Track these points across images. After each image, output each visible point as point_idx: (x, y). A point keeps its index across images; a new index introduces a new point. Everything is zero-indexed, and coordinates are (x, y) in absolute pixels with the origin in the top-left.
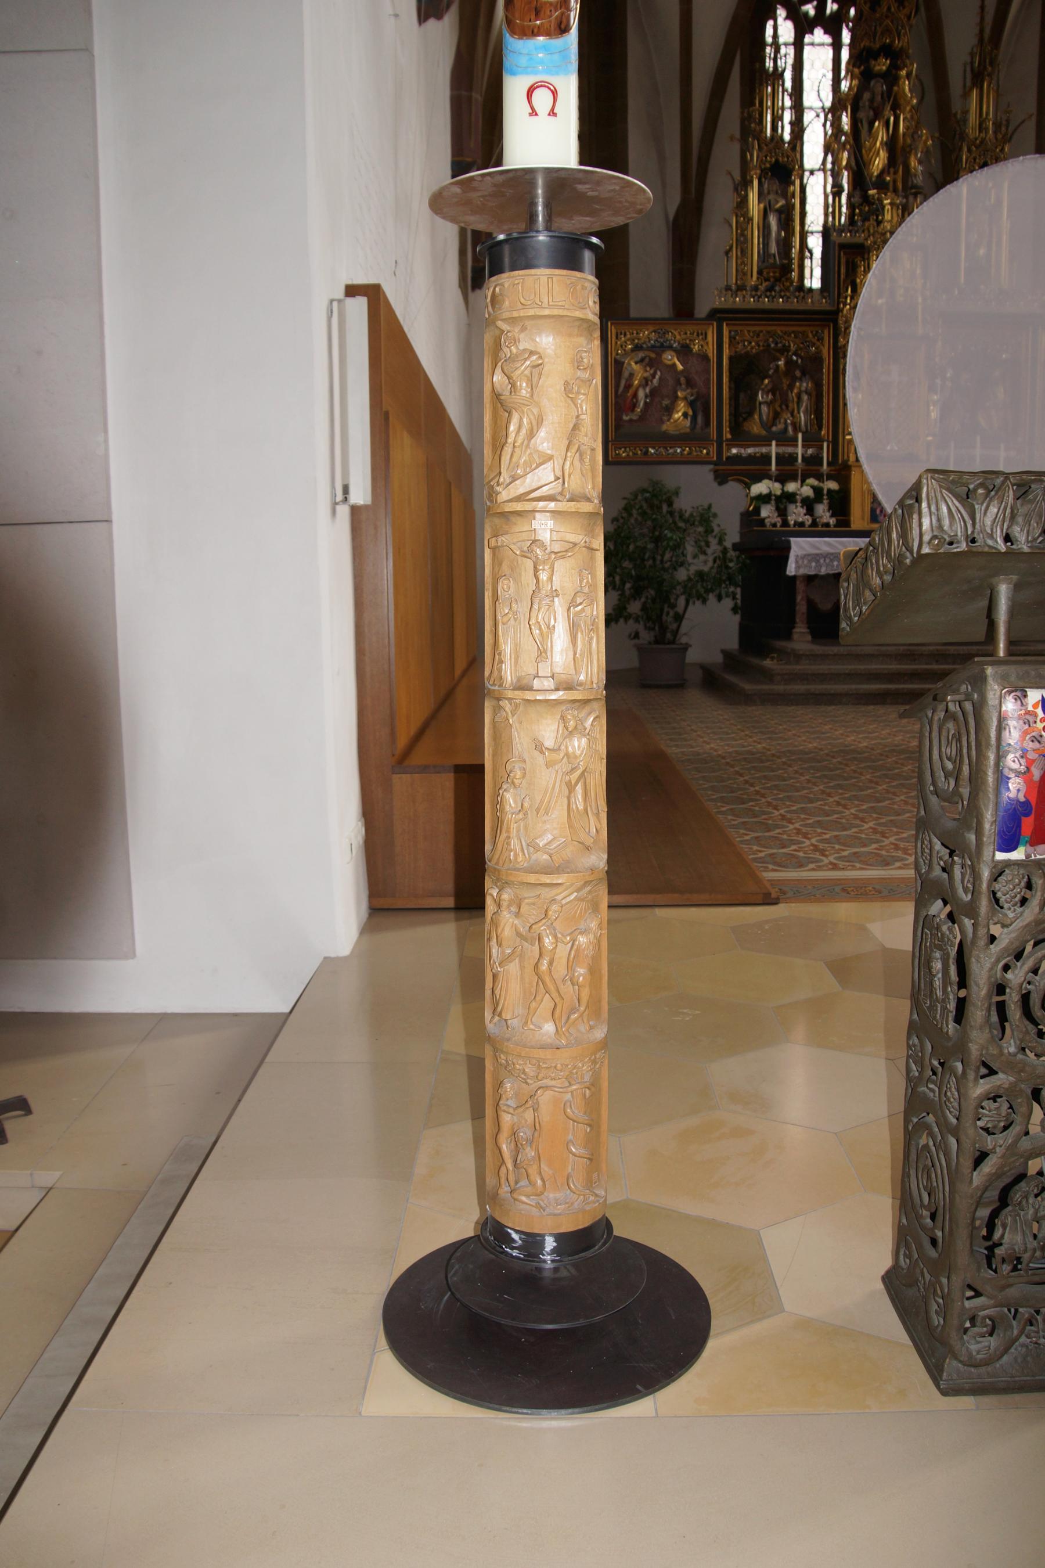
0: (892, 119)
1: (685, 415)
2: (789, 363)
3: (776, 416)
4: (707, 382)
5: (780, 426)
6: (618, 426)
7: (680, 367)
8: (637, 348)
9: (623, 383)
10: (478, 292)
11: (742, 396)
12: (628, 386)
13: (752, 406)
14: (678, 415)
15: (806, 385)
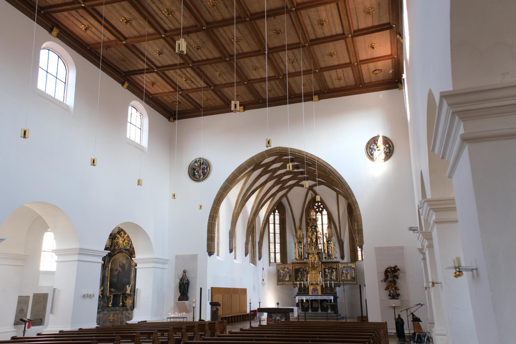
0: (316, 234)
1: (288, 278)
2: (303, 270)
3: (302, 277)
4: (291, 273)
5: (302, 279)
6: (279, 280)
7: (287, 271)
8: (281, 268)
9: (279, 273)
10: (260, 261)
11: (297, 275)
12: (280, 273)
13: (298, 276)
14: (287, 278)
15: (305, 273)
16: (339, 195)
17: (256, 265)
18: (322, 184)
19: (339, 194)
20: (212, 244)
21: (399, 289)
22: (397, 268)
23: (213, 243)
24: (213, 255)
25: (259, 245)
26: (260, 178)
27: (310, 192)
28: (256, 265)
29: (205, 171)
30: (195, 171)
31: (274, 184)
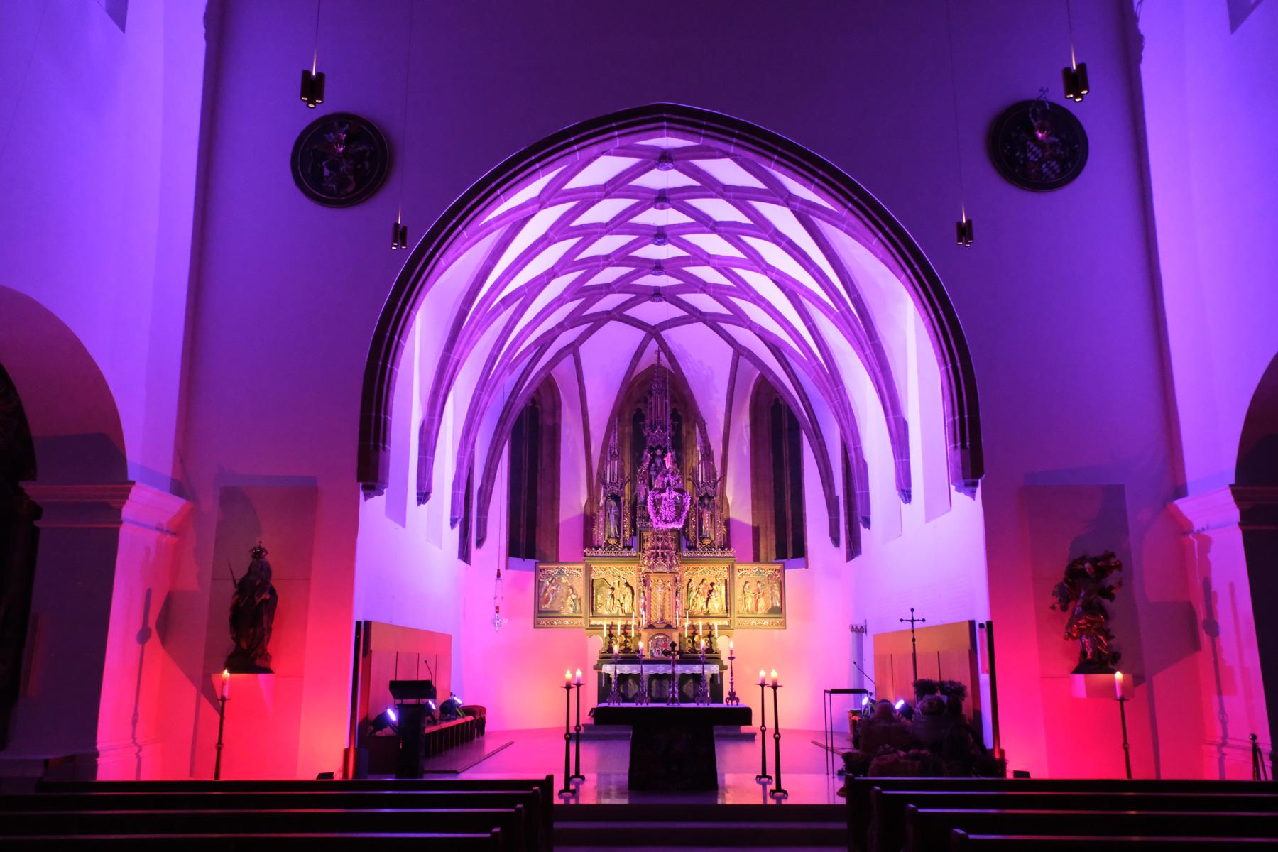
16: (741, 357)
17: (470, 564)
18: (698, 320)
19: (743, 355)
20: (381, 450)
21: (1113, 637)
22: (1113, 562)
23: (384, 449)
24: (381, 493)
25: (482, 499)
26: (545, 248)
27: (654, 345)
28: (470, 564)
29: (367, 164)
30: (324, 163)
31: (562, 295)
